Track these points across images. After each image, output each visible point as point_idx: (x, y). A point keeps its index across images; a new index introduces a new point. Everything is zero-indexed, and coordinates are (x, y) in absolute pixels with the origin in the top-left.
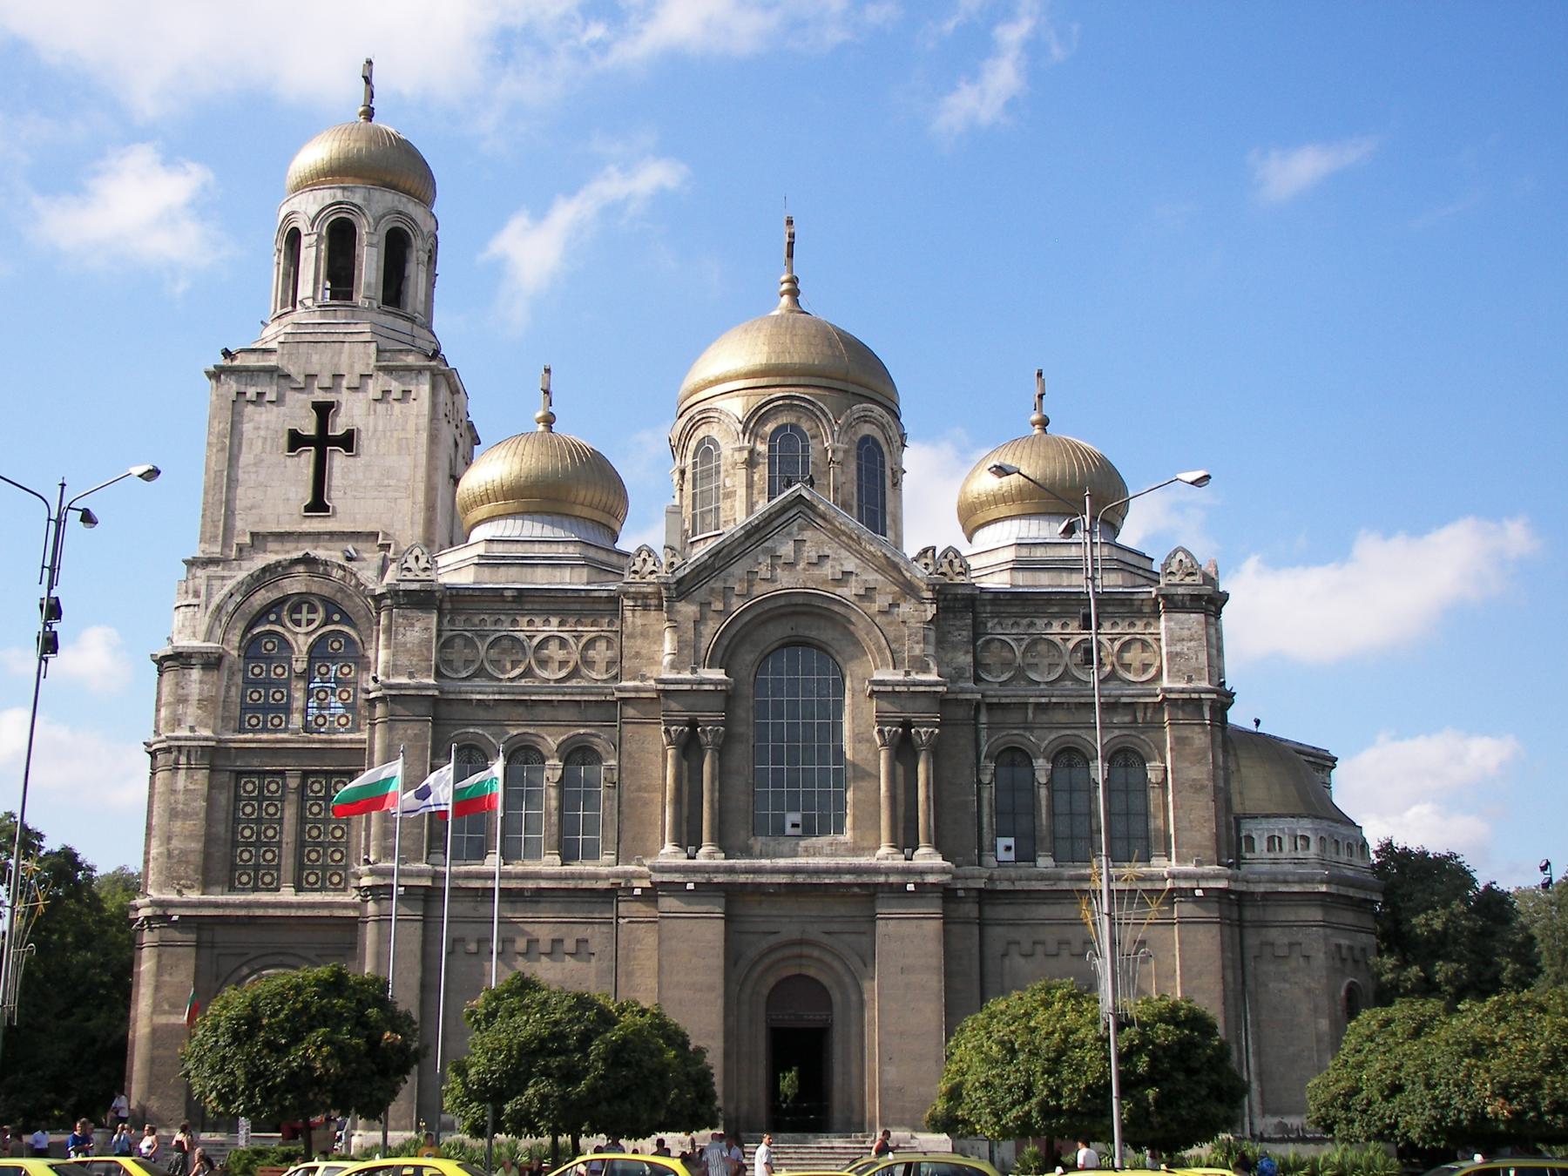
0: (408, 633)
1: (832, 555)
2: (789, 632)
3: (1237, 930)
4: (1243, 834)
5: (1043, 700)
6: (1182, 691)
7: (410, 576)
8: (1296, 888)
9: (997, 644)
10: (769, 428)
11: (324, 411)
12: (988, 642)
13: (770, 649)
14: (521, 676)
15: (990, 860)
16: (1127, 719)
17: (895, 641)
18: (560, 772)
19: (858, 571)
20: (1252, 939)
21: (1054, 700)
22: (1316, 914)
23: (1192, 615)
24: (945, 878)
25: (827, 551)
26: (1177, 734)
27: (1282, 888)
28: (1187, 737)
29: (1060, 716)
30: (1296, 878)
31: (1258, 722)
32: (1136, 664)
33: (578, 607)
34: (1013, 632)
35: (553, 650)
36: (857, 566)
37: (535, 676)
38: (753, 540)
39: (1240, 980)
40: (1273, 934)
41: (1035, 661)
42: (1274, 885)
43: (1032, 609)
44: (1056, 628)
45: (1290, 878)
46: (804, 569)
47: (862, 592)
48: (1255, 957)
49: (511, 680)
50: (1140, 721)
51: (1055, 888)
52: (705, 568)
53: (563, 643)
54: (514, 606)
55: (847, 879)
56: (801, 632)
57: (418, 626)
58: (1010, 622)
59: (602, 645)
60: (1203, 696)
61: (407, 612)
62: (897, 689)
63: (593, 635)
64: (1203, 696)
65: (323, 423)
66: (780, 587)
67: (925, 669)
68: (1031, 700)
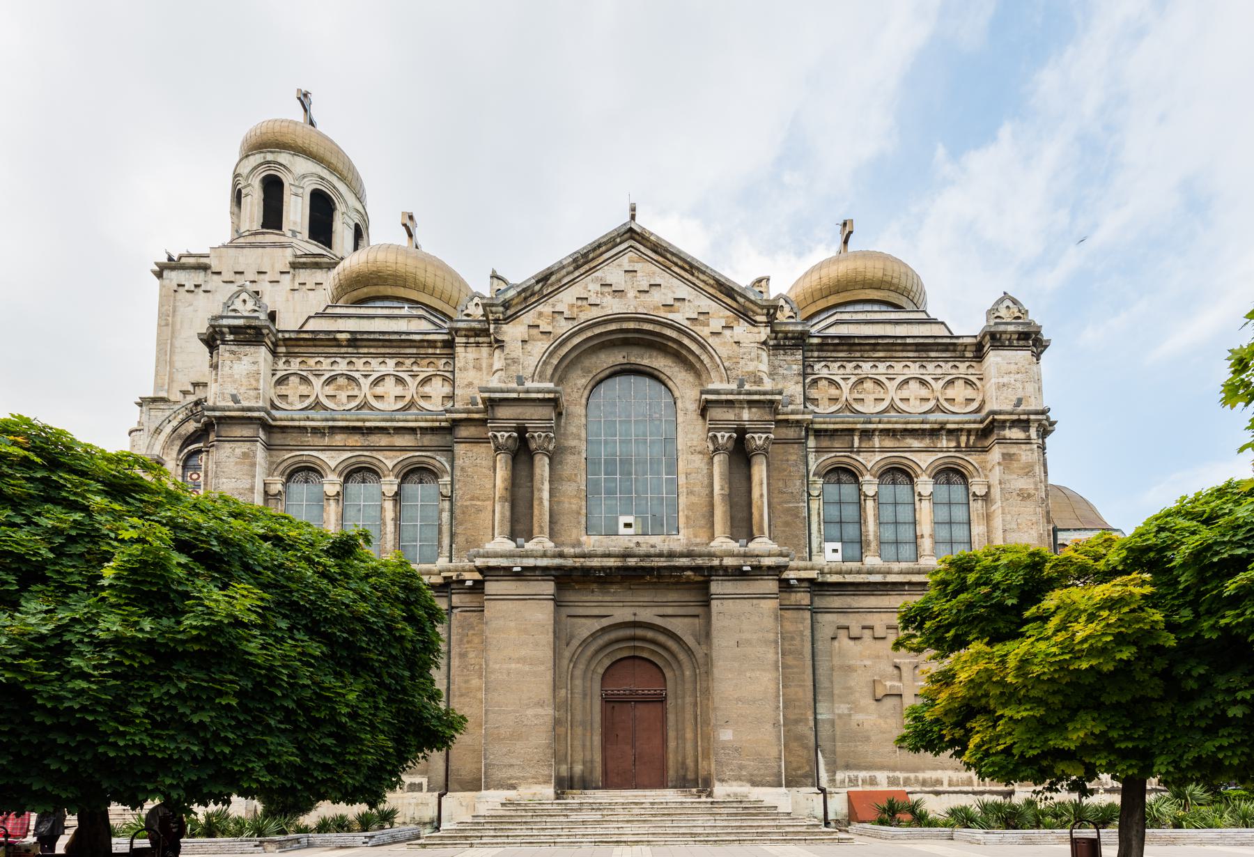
0: (235, 366)
2: (621, 361)
13: (602, 375)
16: (953, 444)
19: (690, 298)
21: (881, 426)
35: (390, 388)
38: (582, 270)
46: (636, 297)
47: (695, 316)
50: (963, 445)
52: (533, 294)
53: (400, 380)
56: (633, 360)
57: (246, 360)
59: (437, 382)
60: (1032, 417)
61: (234, 348)
64: (1032, 417)
66: (610, 312)
68: (859, 426)
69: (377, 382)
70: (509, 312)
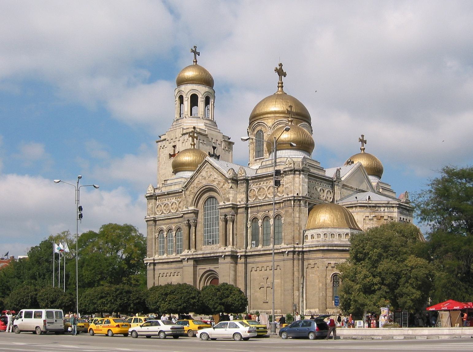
1: (212, 174)
3: (300, 261)
4: (305, 235)
5: (260, 204)
6: (286, 198)
7: (149, 192)
8: (315, 249)
9: (253, 190)
10: (256, 132)
11: (174, 147)
12: (251, 190)
14: (169, 212)
15: (249, 247)
17: (224, 194)
18: (175, 234)
20: (306, 263)
22: (320, 255)
23: (291, 176)
24: (230, 253)
25: (212, 173)
26: (286, 210)
27: (311, 249)
28: (288, 210)
29: (264, 208)
30: (314, 246)
31: (356, 198)
32: (281, 191)
33: (177, 194)
34: (257, 186)
35: (174, 206)
36: (217, 176)
37: (171, 212)
38: (198, 173)
39: (301, 274)
40: (311, 262)
41: (260, 194)
42: (310, 248)
43: (260, 180)
44: (265, 184)
45: (313, 246)
47: (218, 183)
48: (307, 268)
49: (168, 213)
51: (259, 253)
54: (168, 196)
55: (212, 255)
58: (256, 184)
60: (290, 198)
62: (223, 207)
63: (180, 201)
65: (174, 151)
67: (229, 201)
69: (172, 205)
70: (187, 188)
